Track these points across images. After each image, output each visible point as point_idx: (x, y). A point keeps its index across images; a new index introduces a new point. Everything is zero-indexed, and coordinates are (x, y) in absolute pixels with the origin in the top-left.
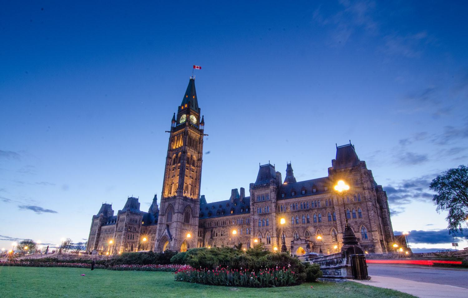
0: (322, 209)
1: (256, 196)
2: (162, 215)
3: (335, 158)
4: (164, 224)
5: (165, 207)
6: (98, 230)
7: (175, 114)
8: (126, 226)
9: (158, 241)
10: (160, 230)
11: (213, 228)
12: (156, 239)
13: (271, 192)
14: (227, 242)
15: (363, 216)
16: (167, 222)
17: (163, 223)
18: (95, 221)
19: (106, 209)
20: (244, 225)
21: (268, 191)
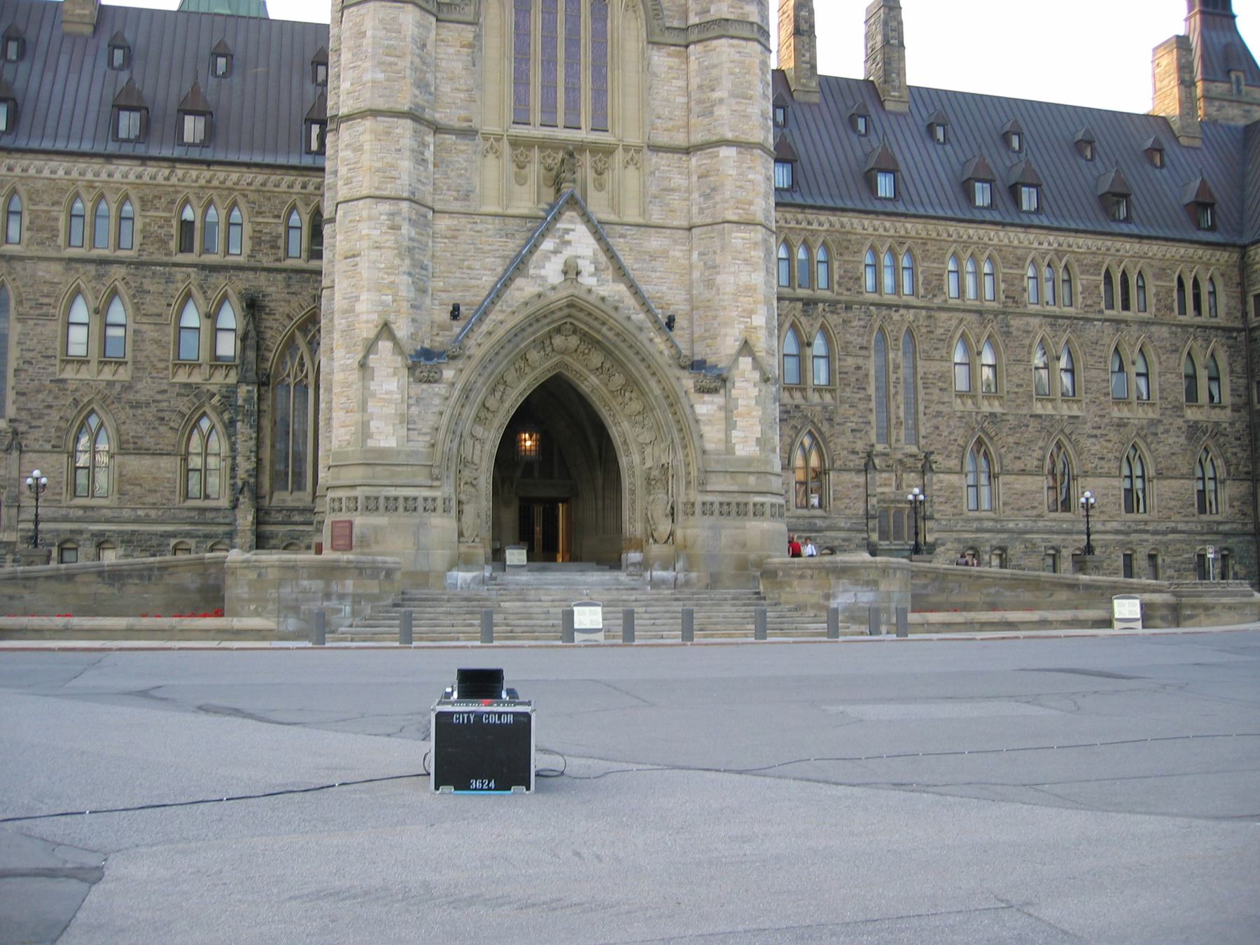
4: (468, 133)
12: (386, 329)
14: (860, 446)
20: (1016, 323)
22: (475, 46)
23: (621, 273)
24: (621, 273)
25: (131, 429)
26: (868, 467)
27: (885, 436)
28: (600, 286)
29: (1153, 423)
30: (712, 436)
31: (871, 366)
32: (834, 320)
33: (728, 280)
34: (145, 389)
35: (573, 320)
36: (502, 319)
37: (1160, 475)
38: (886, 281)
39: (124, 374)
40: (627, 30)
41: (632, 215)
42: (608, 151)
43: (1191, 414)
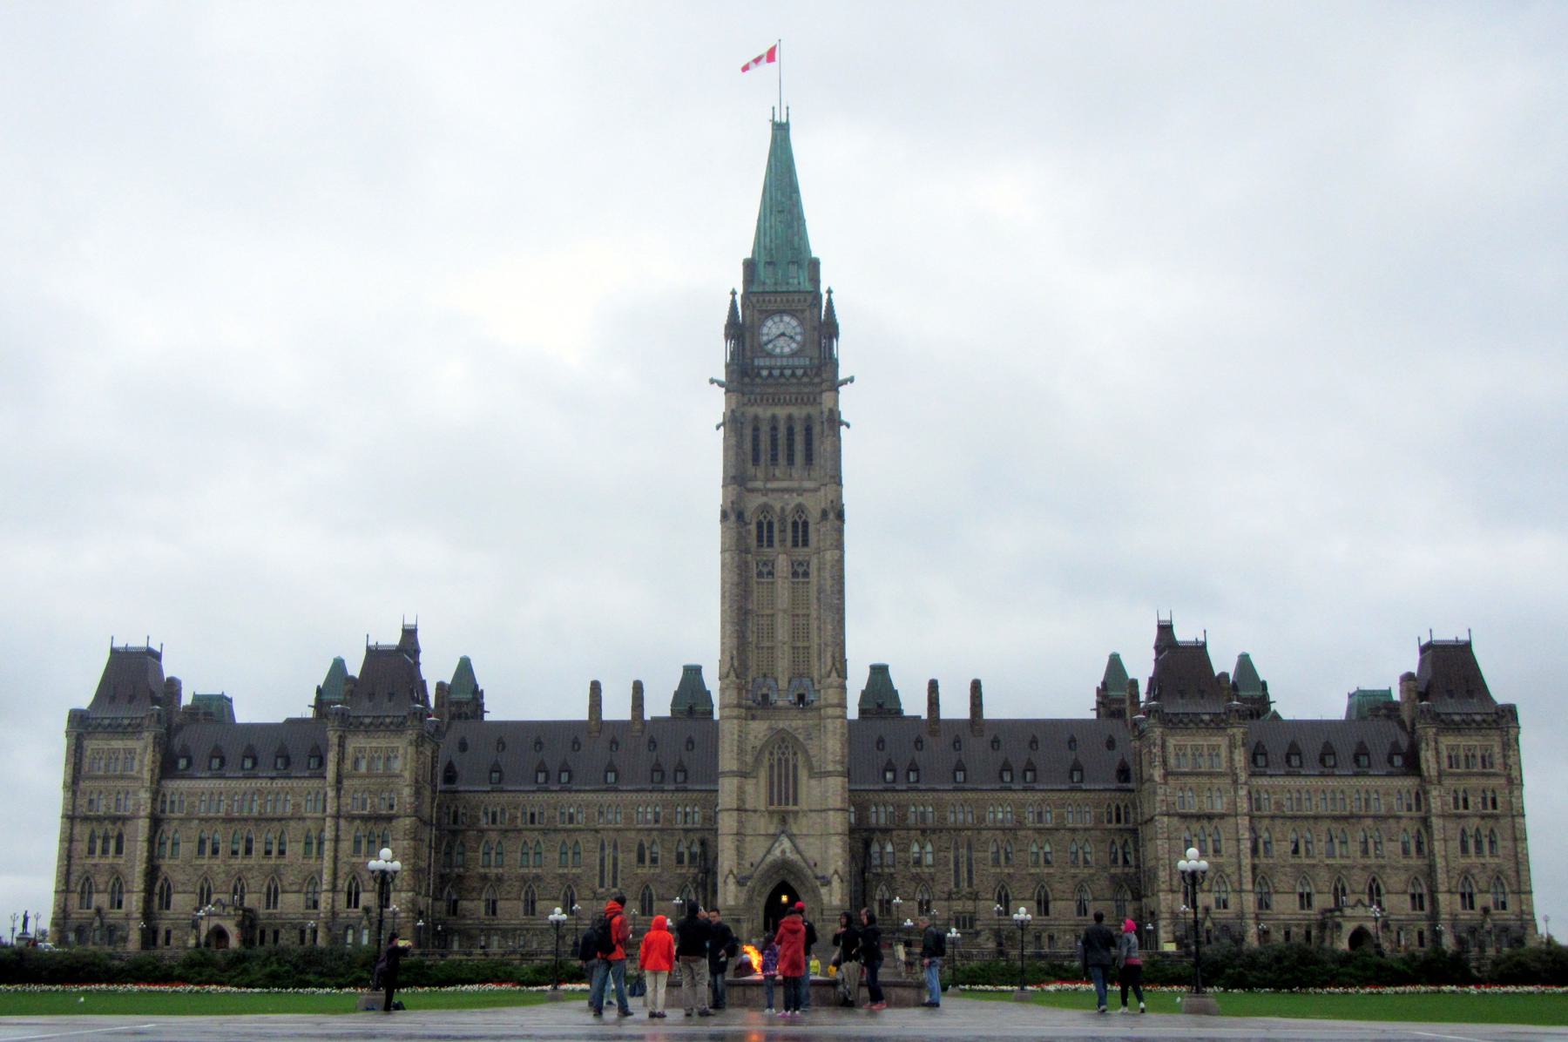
0: (1384, 818)
1: (1171, 749)
2: (742, 775)
3: (1414, 669)
4: (755, 811)
5: (751, 737)
6: (154, 800)
7: (734, 293)
8: (418, 793)
9: (741, 882)
10: (740, 835)
11: (872, 830)
13: (1232, 747)
15: (1500, 852)
16: (772, 804)
17: (747, 807)
18: (91, 745)
19: (133, 677)
20: (1021, 833)
21: (1221, 741)
22: (757, 784)
23: (799, 852)
24: (799, 852)
25: (661, 891)
26: (949, 898)
27: (957, 885)
28: (791, 856)
29: (1092, 875)
30: (826, 899)
31: (951, 856)
32: (934, 837)
33: (831, 852)
34: (666, 876)
35: (784, 865)
36: (763, 866)
37: (1095, 899)
38: (958, 817)
39: (658, 871)
40: (803, 774)
41: (805, 831)
42: (796, 813)
43: (1113, 871)
